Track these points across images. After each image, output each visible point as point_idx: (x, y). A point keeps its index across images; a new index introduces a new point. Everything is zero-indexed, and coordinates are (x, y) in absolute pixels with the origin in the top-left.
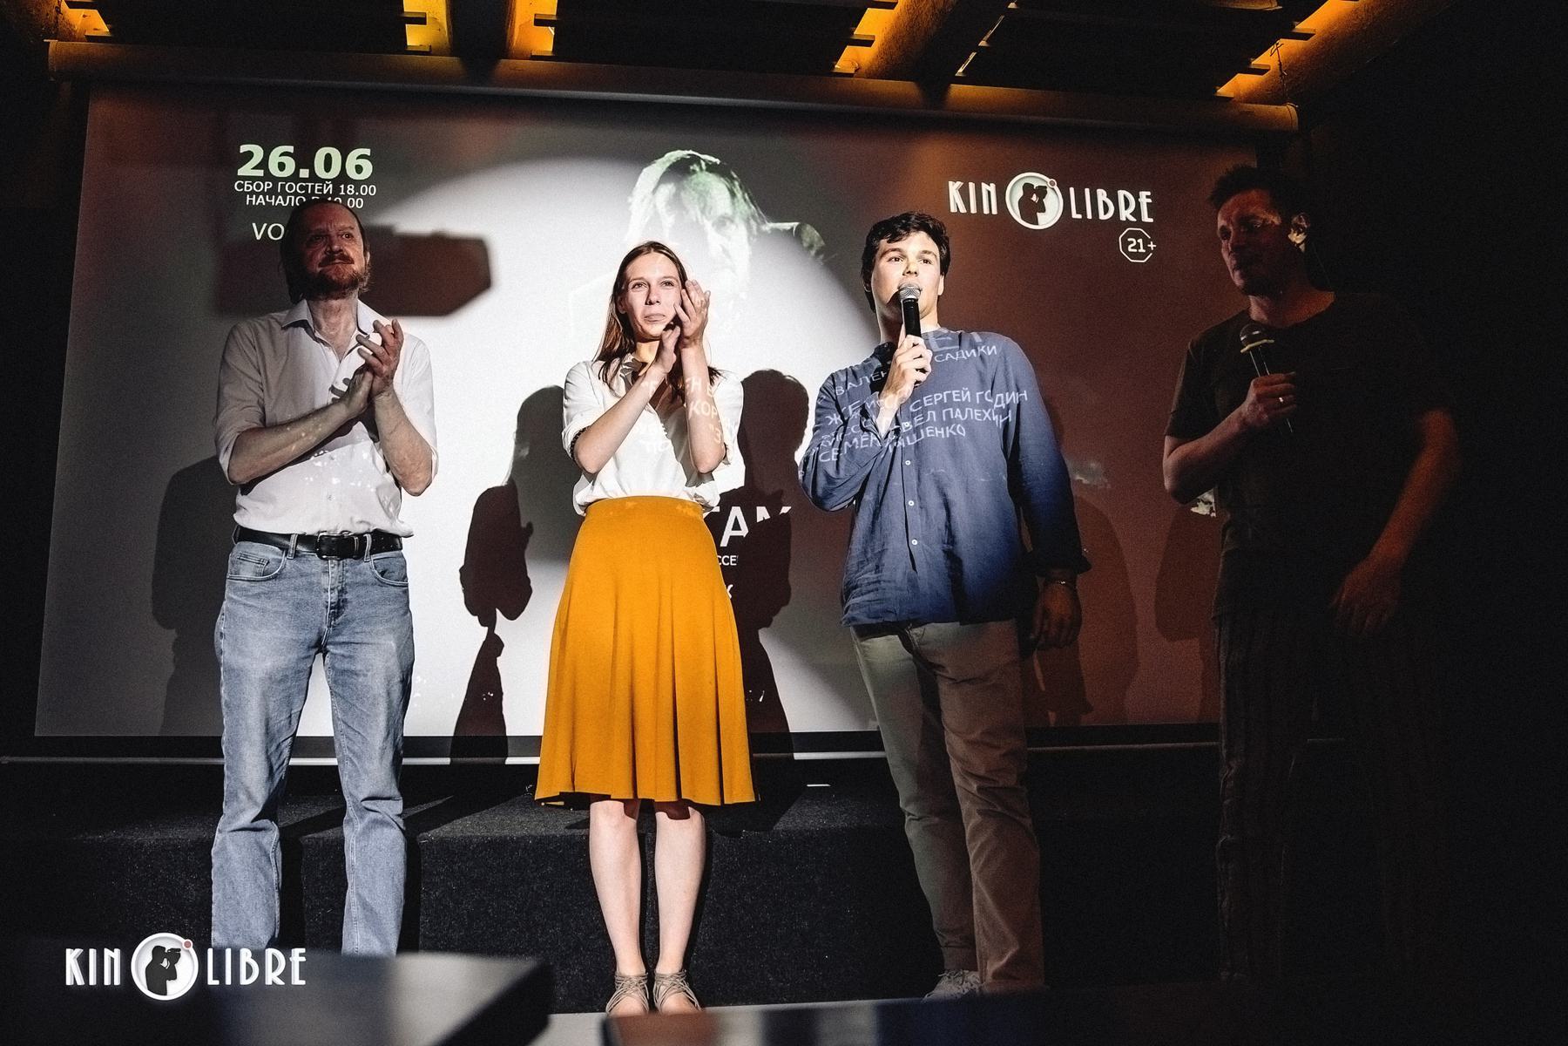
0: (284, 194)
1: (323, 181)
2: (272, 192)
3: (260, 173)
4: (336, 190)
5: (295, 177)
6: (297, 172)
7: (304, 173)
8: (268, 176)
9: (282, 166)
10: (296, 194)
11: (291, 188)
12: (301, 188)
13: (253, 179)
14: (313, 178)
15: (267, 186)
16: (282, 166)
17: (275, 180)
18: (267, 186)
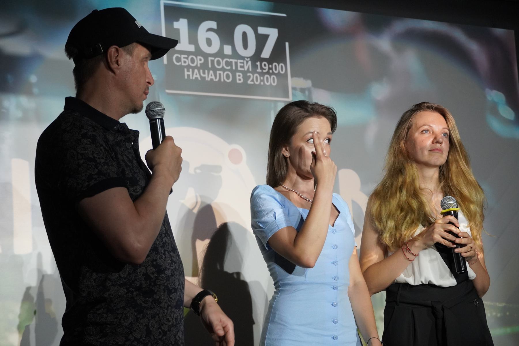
0: (215, 70)
1: (243, 58)
2: (204, 67)
3: (191, 48)
4: (254, 66)
5: (220, 54)
6: (221, 49)
7: (228, 50)
8: (198, 52)
9: (209, 42)
10: (223, 70)
11: (219, 63)
12: (228, 64)
13: (188, 53)
14: (235, 54)
15: (199, 61)
16: (209, 42)
17: (206, 56)
18: (199, 61)
